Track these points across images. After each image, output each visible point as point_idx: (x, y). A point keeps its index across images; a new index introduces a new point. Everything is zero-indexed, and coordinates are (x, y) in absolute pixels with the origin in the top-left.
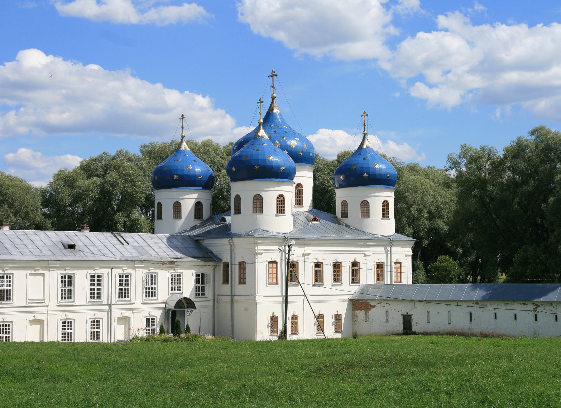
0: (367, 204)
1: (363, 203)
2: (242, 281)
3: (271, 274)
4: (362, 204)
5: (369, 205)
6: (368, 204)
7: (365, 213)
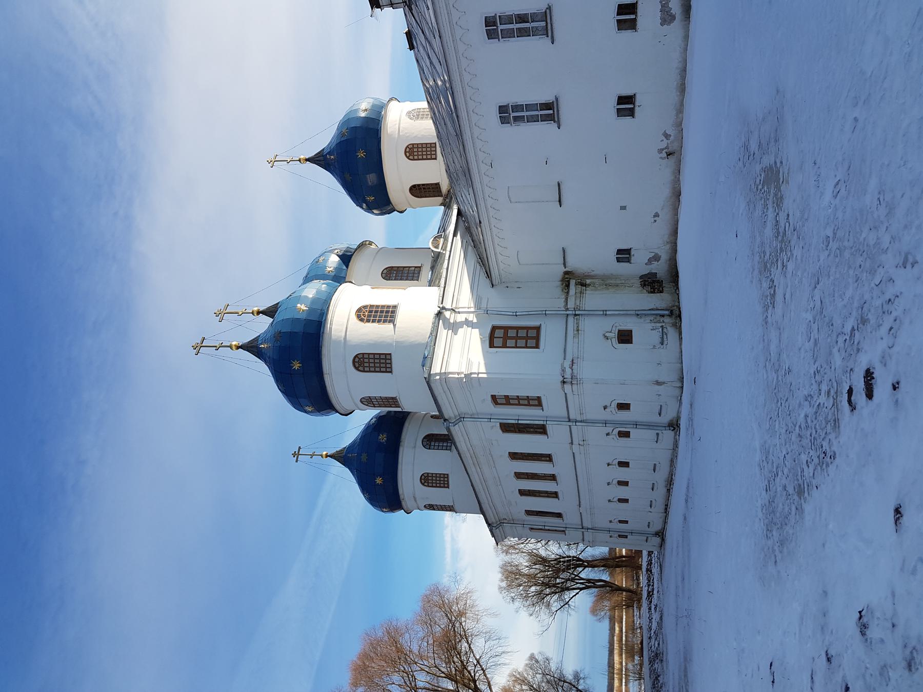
0: (410, 149)
2: (536, 402)
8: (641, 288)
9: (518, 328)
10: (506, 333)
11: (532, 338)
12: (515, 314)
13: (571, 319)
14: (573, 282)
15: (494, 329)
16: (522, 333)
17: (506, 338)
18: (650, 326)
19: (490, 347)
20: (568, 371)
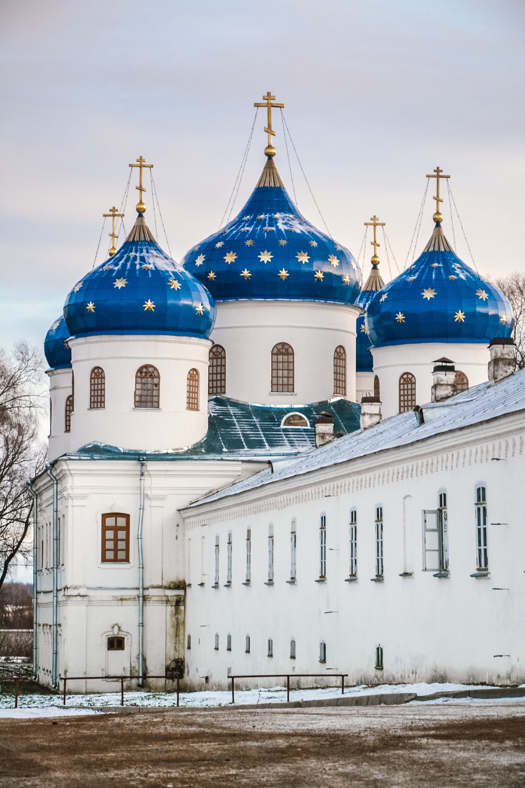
0: (411, 380)
1: (405, 380)
3: (112, 542)
4: (402, 381)
5: (415, 383)
6: (413, 381)
7: (408, 401)
8: (173, 658)
9: (127, 540)
10: (121, 528)
11: (116, 555)
12: (139, 537)
13: (135, 593)
14: (181, 592)
15: (127, 516)
16: (121, 545)
17: (116, 529)
18: (127, 666)
19: (103, 515)
20: (75, 592)
